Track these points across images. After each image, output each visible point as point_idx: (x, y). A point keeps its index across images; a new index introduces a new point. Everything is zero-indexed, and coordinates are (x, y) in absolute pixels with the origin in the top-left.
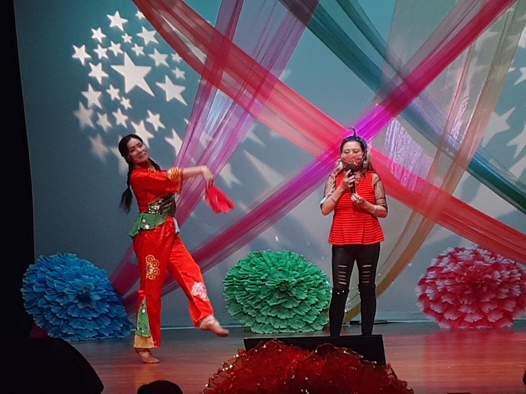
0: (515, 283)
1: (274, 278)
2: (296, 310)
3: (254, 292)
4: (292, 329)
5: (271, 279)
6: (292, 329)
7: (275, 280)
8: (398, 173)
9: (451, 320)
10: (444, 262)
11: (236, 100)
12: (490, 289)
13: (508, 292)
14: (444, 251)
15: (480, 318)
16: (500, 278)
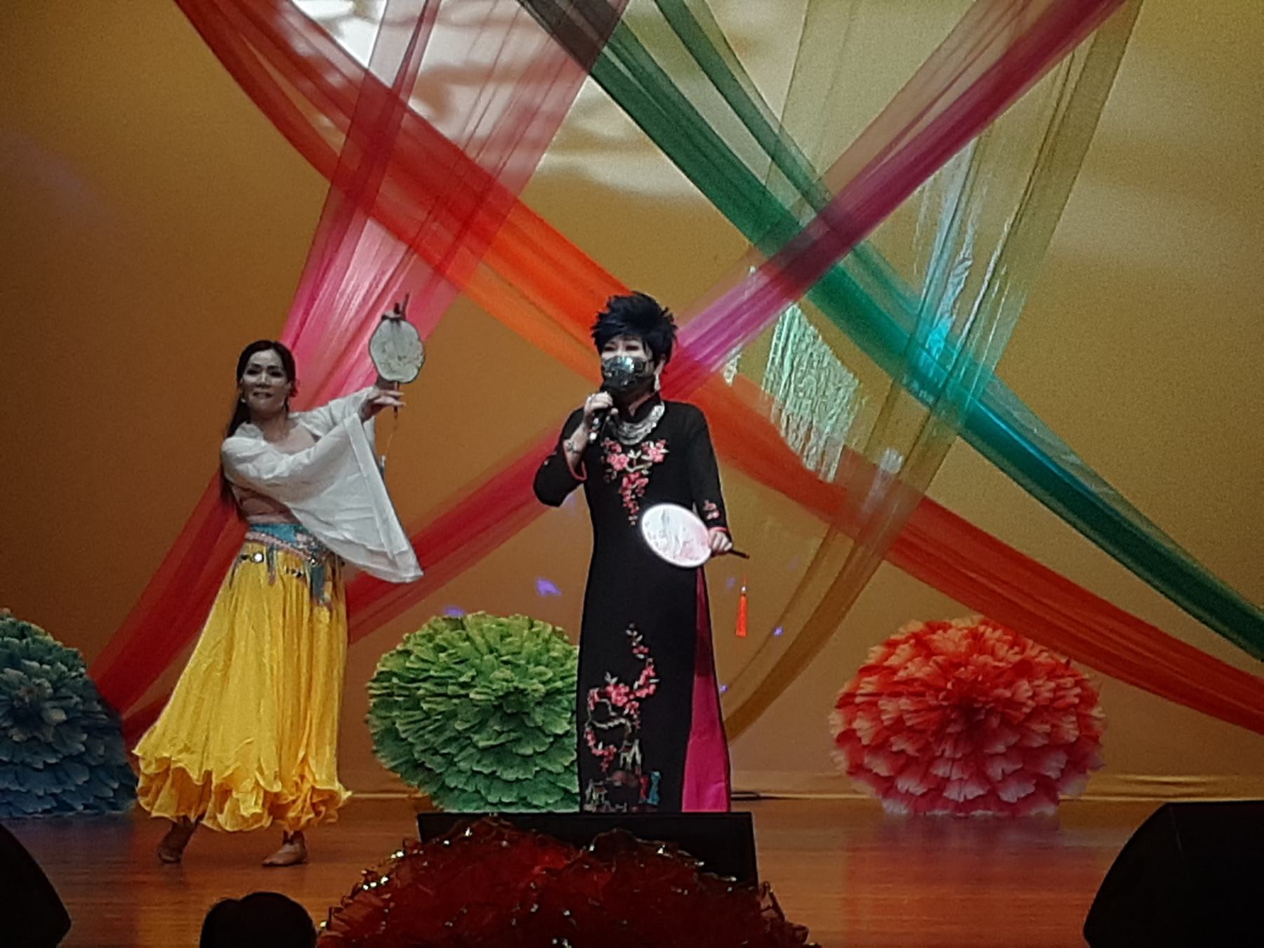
0: (1067, 710)
1: (491, 682)
2: (543, 759)
3: (440, 713)
4: (529, 805)
5: (487, 684)
6: (529, 805)
7: (494, 687)
8: (797, 437)
9: (912, 795)
10: (898, 655)
11: (414, 246)
12: (1006, 722)
13: (1049, 731)
14: (901, 630)
15: (981, 792)
16: (1030, 698)
